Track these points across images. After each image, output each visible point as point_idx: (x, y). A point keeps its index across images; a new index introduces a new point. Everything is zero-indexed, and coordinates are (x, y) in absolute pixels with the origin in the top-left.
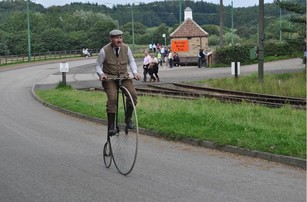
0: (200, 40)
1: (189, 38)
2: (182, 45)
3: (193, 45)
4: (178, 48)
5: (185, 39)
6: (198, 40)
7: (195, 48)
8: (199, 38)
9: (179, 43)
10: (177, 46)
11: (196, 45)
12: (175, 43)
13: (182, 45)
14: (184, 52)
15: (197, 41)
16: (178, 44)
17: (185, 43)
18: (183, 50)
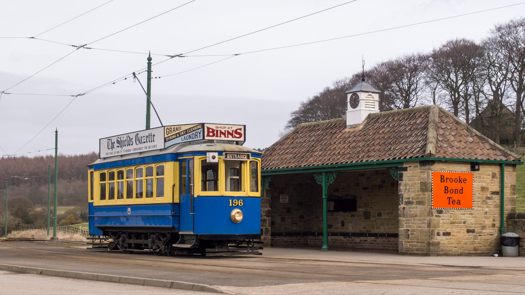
0: (498, 175)
1: (474, 165)
2: (458, 186)
3: (483, 189)
4: (449, 195)
5: (465, 169)
6: (494, 176)
7: (489, 201)
8: (496, 170)
9: (451, 180)
10: (446, 189)
11: (490, 190)
12: (442, 178)
13: (458, 186)
14: (462, 212)
15: (493, 177)
16: (448, 184)
17: (465, 180)
18: (459, 203)
